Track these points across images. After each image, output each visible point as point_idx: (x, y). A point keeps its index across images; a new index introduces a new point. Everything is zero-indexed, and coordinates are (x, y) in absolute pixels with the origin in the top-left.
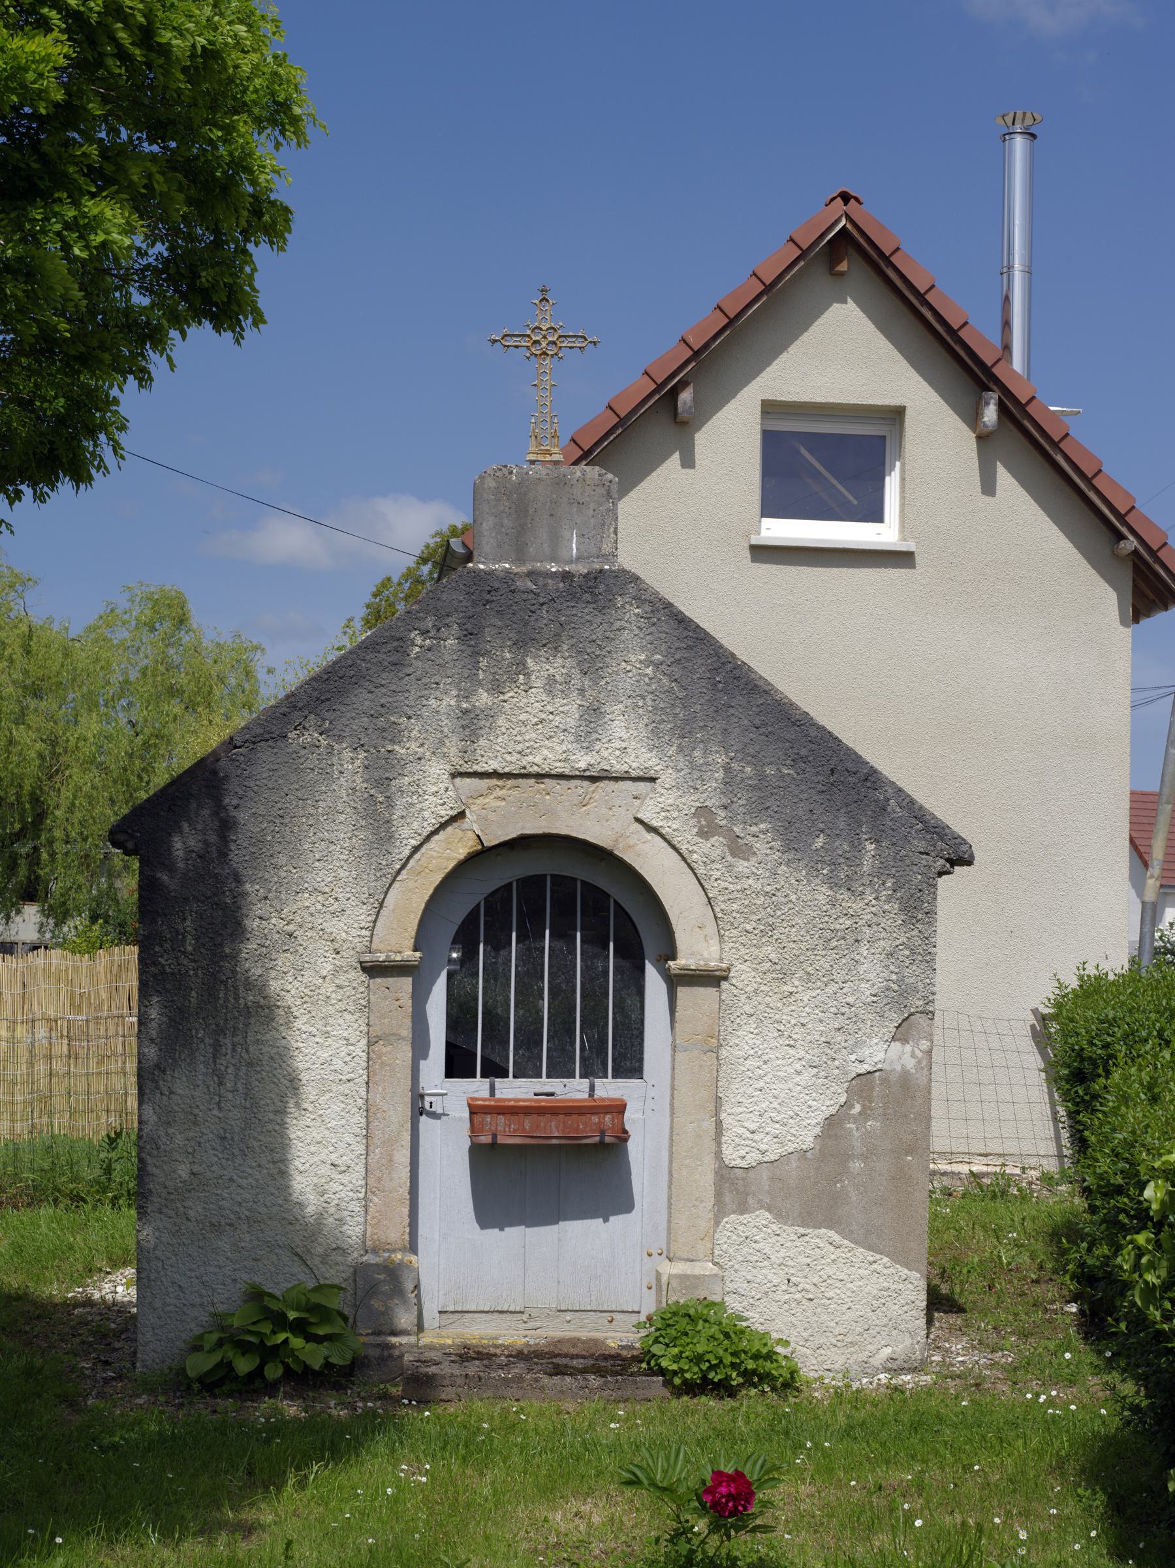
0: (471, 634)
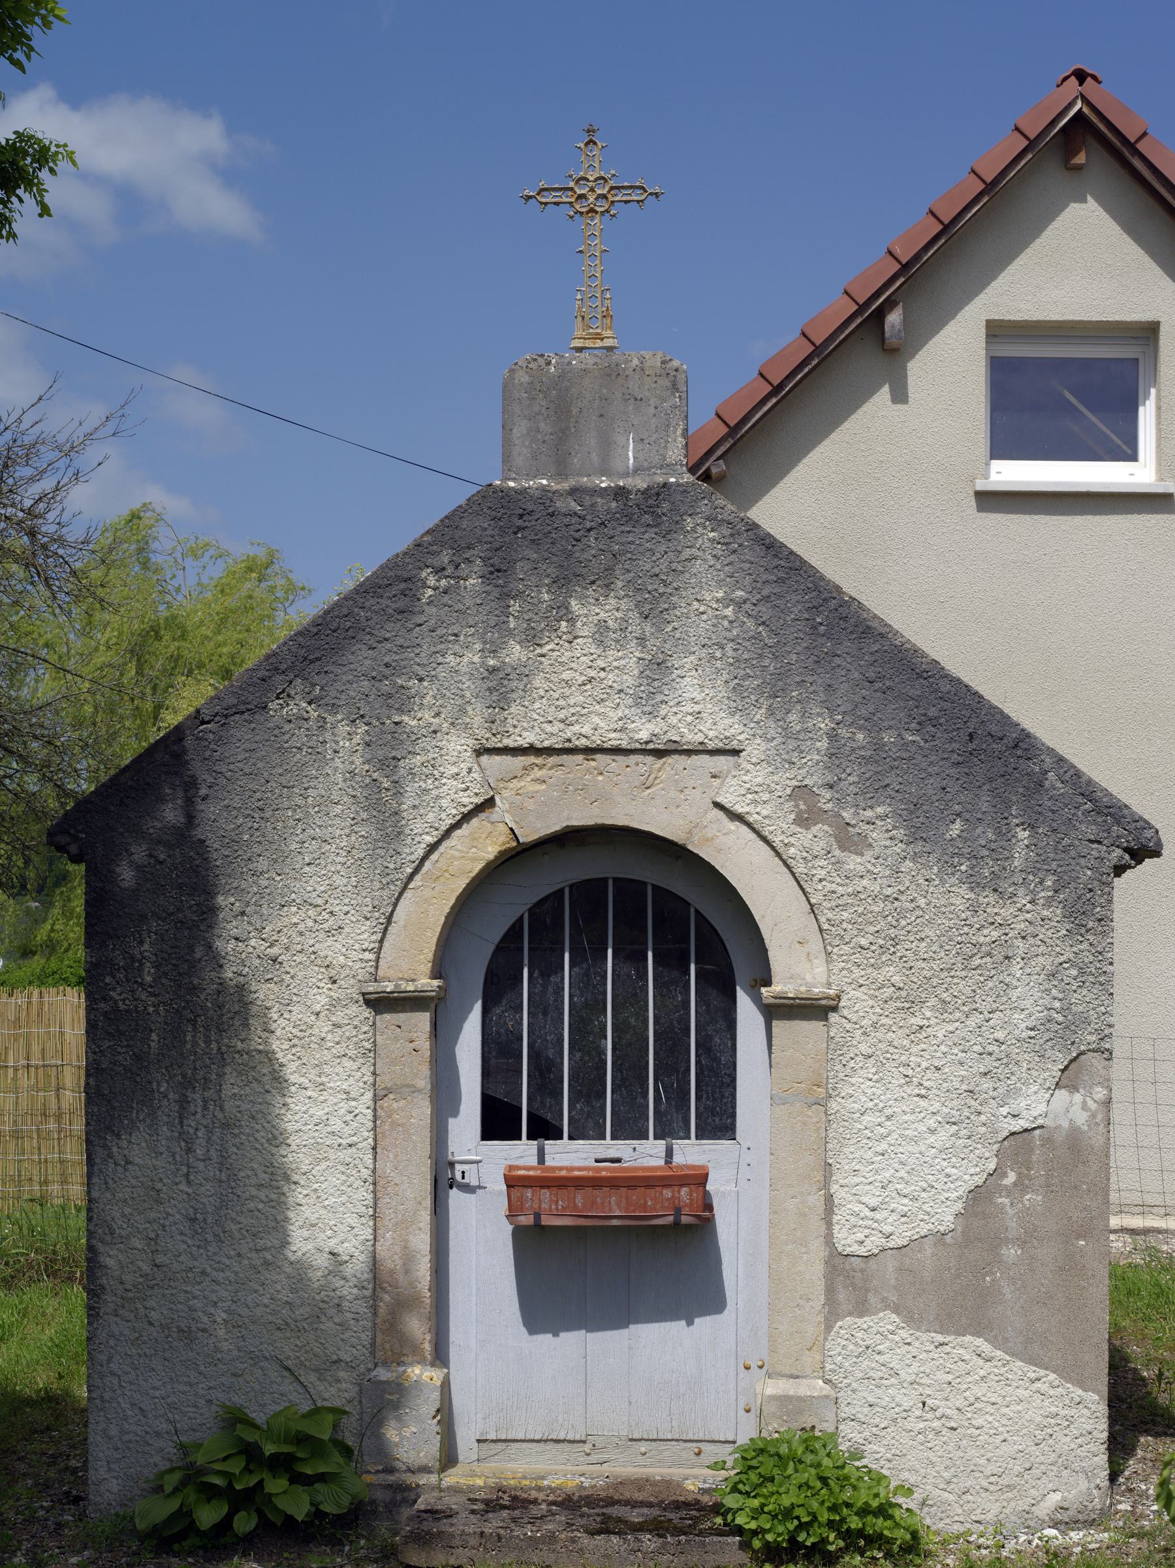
0: (499, 571)
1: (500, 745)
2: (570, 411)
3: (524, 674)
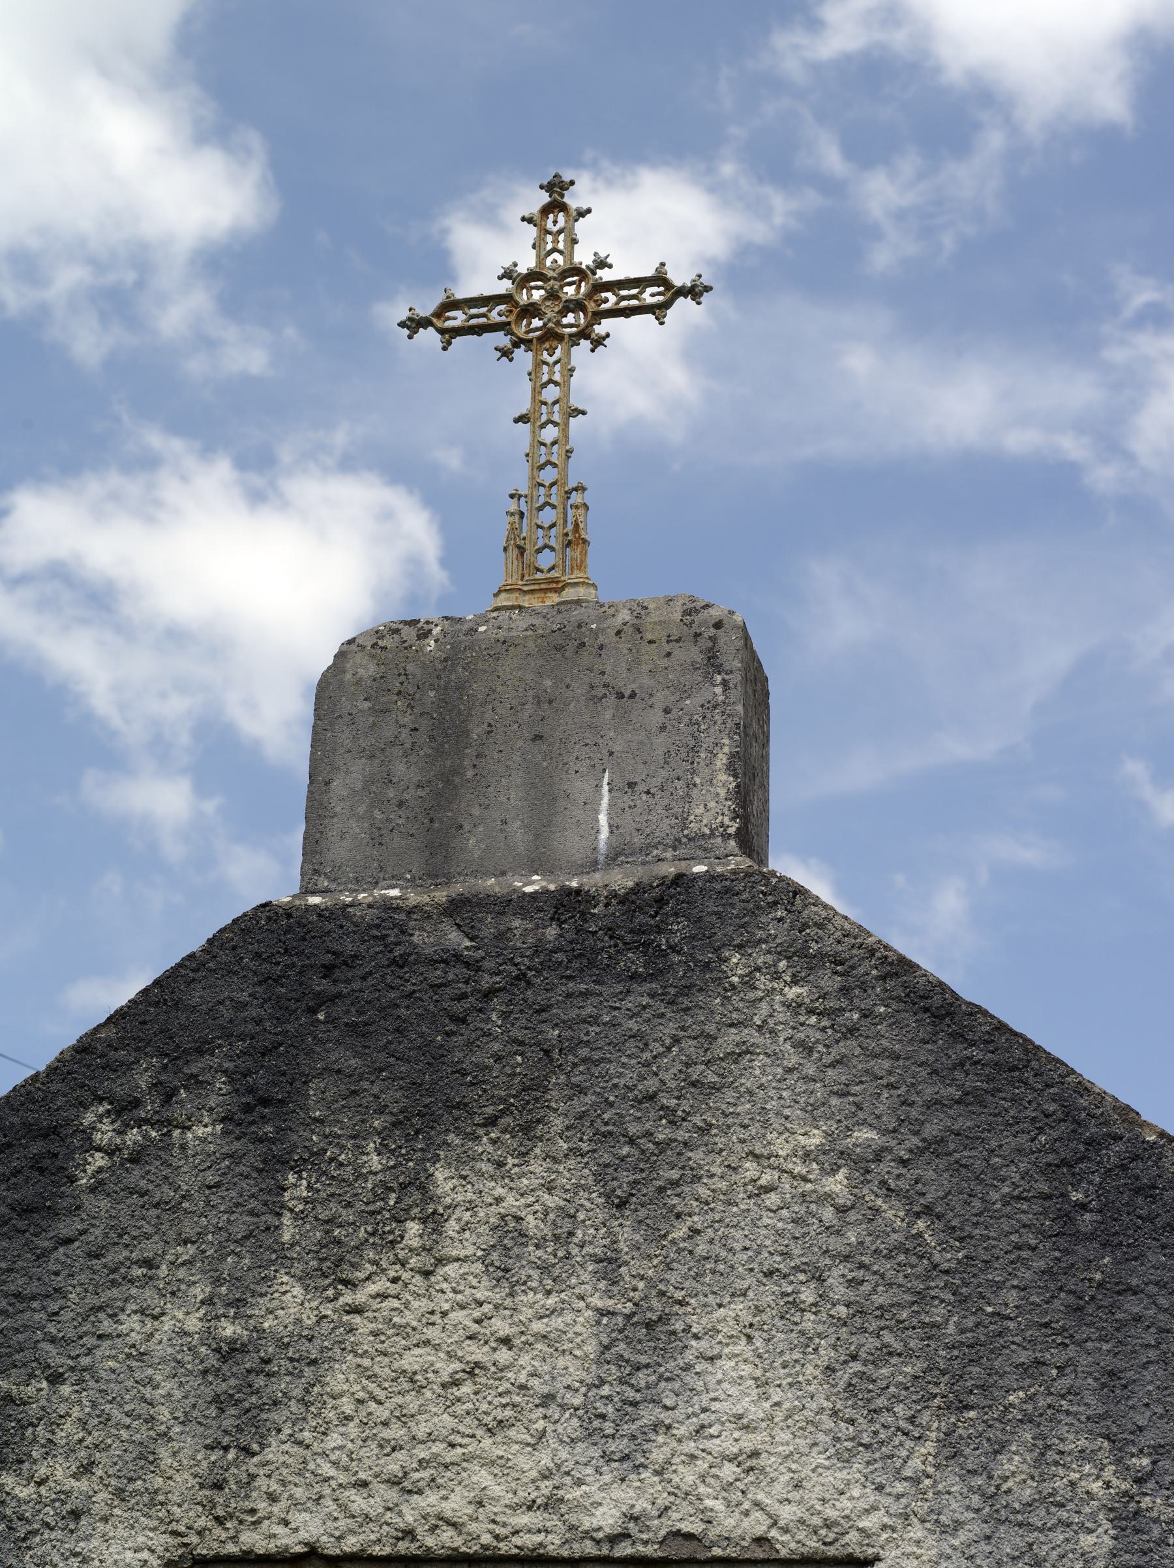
0: (265, 1102)
1: (231, 1549)
2: (467, 733)
3: (307, 1357)
